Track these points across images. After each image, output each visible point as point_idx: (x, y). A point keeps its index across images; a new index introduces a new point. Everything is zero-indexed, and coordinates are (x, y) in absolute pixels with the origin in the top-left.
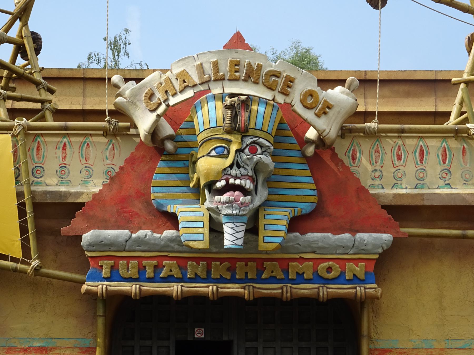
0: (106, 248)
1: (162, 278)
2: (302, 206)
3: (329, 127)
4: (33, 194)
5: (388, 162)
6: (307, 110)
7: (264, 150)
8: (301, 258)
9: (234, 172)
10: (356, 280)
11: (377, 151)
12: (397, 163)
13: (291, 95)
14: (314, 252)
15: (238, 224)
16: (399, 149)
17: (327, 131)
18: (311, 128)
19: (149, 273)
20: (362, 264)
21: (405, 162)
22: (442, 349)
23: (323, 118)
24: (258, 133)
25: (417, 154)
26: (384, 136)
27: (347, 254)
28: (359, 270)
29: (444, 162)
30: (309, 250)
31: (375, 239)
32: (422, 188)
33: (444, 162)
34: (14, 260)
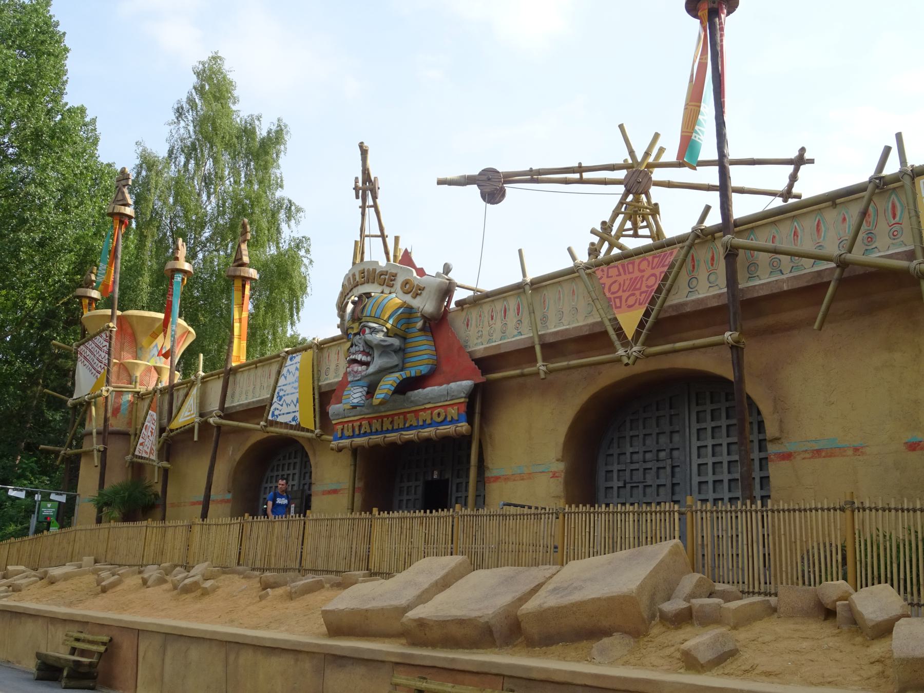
0: (337, 417)
1: (363, 434)
2: (421, 368)
3: (423, 305)
4: (320, 387)
5: (486, 323)
6: (406, 295)
7: (372, 330)
8: (425, 408)
9: (353, 350)
10: (452, 421)
11: (480, 316)
12: (491, 322)
13: (395, 286)
14: (430, 403)
15: (355, 388)
16: (492, 311)
17: (421, 307)
18: (110, 310)
19: (357, 432)
20: (456, 407)
21: (496, 320)
22: (530, 474)
23: (418, 298)
24: (368, 319)
25: (503, 312)
26: (447, 304)
27: (447, 401)
28: (453, 412)
29: (518, 315)
30: (426, 401)
31: (458, 386)
32: (504, 339)
33: (518, 315)
34: (308, 430)
